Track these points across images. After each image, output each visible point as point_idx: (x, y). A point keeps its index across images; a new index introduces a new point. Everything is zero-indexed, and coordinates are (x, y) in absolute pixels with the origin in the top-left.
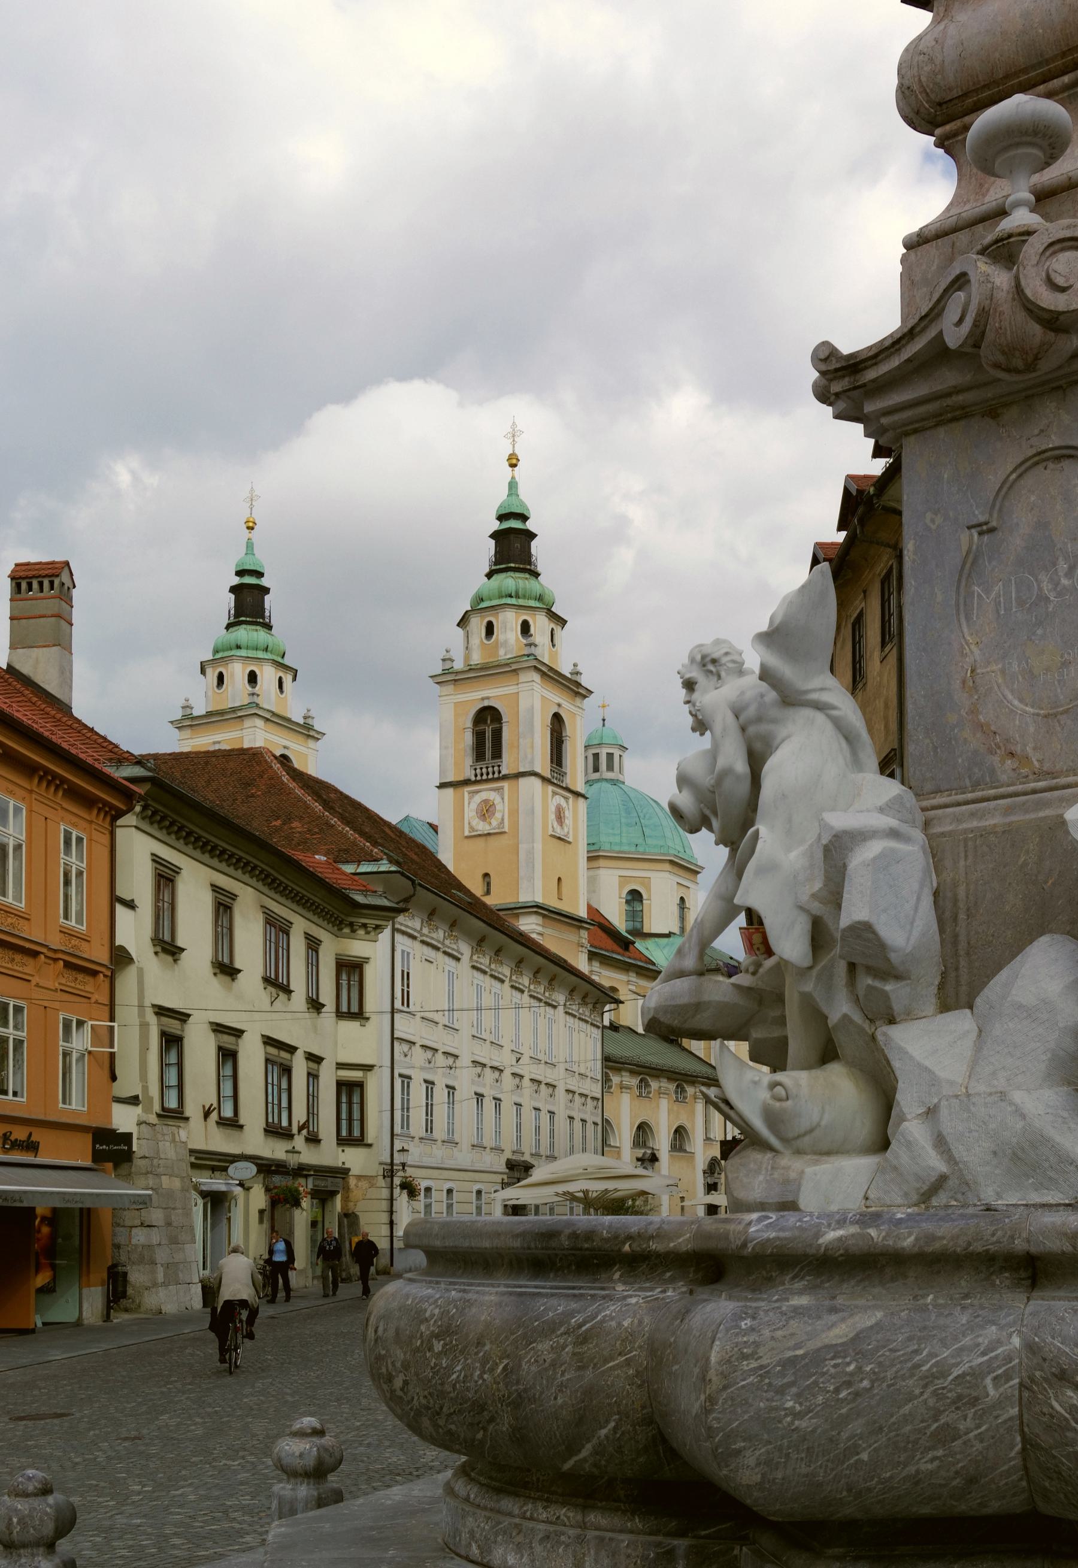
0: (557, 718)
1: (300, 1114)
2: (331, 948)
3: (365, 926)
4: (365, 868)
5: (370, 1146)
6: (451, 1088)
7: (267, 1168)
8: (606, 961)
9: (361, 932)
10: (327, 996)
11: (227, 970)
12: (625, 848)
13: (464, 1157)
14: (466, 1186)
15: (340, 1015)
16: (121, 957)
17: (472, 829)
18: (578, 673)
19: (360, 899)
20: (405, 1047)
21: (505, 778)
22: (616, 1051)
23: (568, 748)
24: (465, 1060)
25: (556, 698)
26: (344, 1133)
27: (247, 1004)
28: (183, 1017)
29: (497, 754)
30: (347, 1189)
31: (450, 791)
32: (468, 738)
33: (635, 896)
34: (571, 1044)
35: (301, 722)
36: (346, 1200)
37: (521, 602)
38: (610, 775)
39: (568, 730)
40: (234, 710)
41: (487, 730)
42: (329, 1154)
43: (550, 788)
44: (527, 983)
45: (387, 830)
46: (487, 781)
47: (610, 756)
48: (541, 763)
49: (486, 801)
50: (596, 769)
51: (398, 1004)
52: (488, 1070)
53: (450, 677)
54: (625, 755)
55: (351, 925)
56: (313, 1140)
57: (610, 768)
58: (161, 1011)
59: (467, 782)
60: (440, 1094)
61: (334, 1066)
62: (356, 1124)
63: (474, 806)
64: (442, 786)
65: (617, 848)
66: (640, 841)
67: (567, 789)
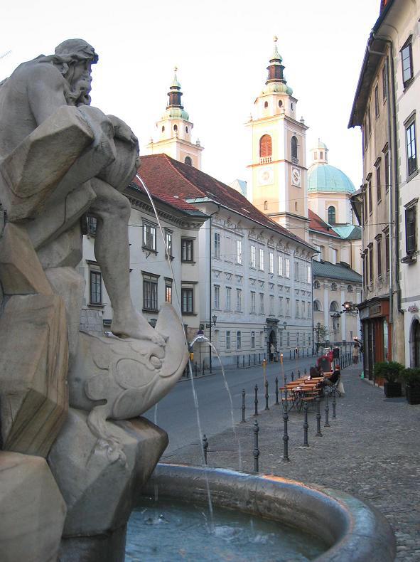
0: (294, 138)
2: (178, 234)
3: (193, 224)
4: (198, 200)
5: (196, 315)
8: (319, 235)
9: (192, 227)
12: (328, 189)
13: (246, 318)
15: (183, 261)
18: (303, 120)
20: (217, 274)
21: (273, 162)
24: (246, 277)
25: (293, 130)
26: (185, 310)
33: (332, 209)
35: (195, 144)
38: (321, 161)
41: (265, 145)
44: (275, 245)
45: (218, 185)
50: (316, 159)
51: (213, 256)
52: (257, 282)
54: (328, 153)
55: (188, 224)
57: (321, 158)
61: (180, 283)
62: (190, 307)
65: (323, 190)
67: (301, 167)
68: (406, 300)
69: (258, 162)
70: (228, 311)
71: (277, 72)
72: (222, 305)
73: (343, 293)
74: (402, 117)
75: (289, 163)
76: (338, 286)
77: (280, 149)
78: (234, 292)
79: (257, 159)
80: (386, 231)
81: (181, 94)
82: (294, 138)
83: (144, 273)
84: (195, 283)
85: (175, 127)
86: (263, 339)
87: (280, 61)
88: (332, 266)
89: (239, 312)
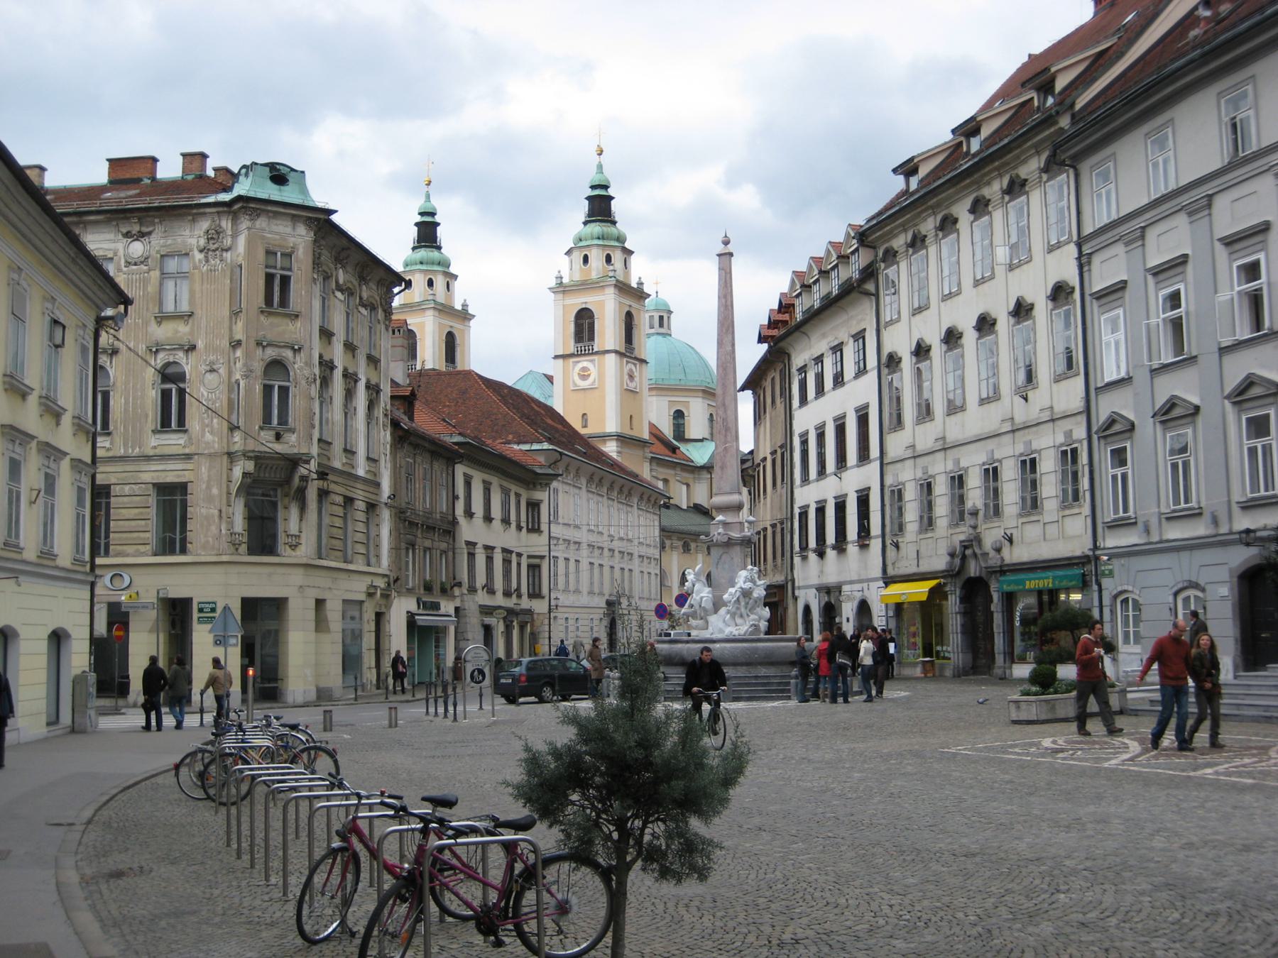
0: (629, 316)
1: (514, 585)
4: (536, 446)
6: (577, 561)
7: (511, 612)
11: (488, 518)
13: (584, 600)
14: (586, 616)
15: (529, 531)
16: (454, 522)
17: (575, 385)
19: (539, 471)
21: (597, 353)
23: (635, 332)
27: (501, 537)
28: (474, 544)
29: (592, 338)
30: (533, 620)
31: (560, 361)
32: (571, 328)
33: (679, 415)
34: (641, 527)
36: (532, 626)
38: (661, 330)
39: (636, 321)
40: (419, 304)
41: (584, 324)
42: (525, 603)
49: (584, 369)
50: (652, 327)
53: (561, 289)
56: (519, 596)
58: (468, 543)
59: (572, 355)
60: (572, 564)
64: (556, 357)
66: (682, 376)
67: (636, 359)
69: (571, 348)
70: (566, 590)
71: (600, 207)
72: (561, 584)
73: (700, 556)
74: (798, 429)
76: (693, 545)
77: (608, 333)
78: (572, 564)
79: (571, 348)
80: (782, 523)
81: (438, 224)
83: (505, 550)
84: (542, 557)
85: (430, 283)
86: (603, 629)
87: (606, 187)
88: (682, 513)
89: (577, 591)
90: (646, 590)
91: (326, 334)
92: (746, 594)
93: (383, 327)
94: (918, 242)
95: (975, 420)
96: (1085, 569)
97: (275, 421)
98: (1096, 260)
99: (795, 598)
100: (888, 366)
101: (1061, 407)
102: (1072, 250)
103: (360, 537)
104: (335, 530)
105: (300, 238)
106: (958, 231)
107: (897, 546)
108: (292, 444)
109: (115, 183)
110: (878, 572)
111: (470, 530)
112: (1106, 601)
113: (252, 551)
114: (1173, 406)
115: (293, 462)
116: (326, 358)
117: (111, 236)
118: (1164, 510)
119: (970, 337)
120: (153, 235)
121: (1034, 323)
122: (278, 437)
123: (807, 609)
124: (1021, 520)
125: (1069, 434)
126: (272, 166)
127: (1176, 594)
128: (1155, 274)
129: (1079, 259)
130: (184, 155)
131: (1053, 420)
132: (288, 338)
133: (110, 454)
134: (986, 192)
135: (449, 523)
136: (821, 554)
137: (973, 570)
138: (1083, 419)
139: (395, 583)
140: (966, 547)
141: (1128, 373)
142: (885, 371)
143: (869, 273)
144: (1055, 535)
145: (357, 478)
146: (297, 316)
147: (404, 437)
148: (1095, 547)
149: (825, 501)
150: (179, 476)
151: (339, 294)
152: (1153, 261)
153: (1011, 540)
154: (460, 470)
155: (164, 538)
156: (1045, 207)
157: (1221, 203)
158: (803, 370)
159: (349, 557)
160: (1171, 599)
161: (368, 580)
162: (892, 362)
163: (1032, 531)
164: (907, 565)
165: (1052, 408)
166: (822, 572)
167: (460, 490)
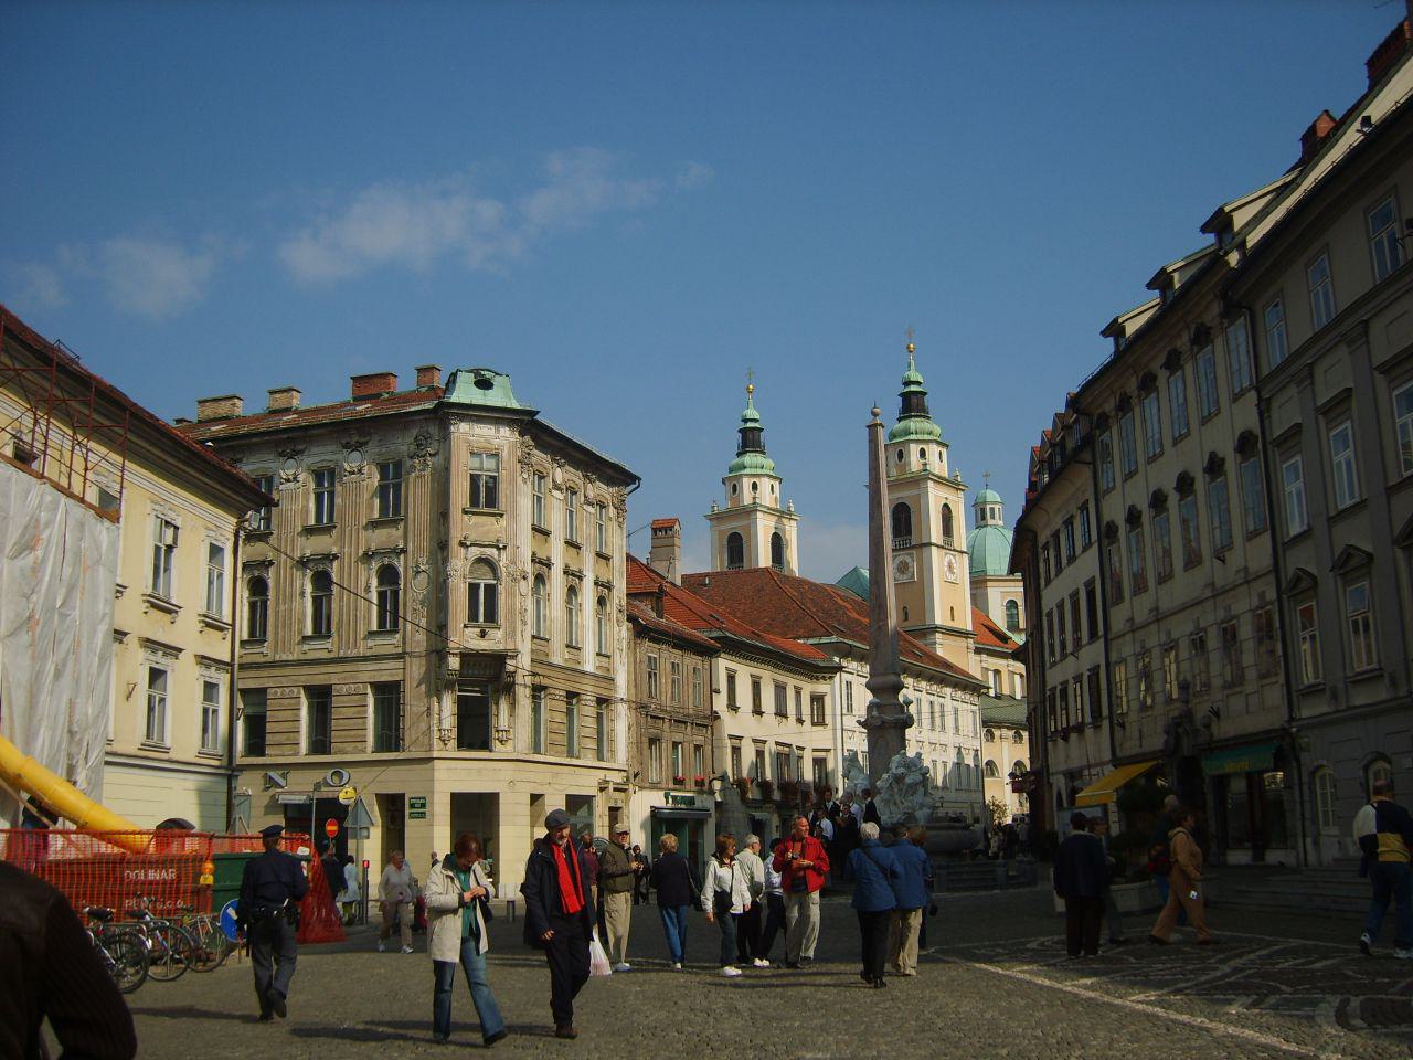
0: (946, 505)
2: (808, 688)
4: (825, 640)
10: (806, 716)
11: (758, 711)
15: (813, 724)
16: (715, 717)
20: (850, 734)
22: (996, 714)
28: (740, 738)
29: (909, 532)
37: (920, 437)
43: (944, 551)
46: (903, 549)
47: (992, 509)
48: (936, 534)
58: (731, 737)
63: (896, 566)
67: (954, 550)
68: (1053, 774)
74: (1045, 612)
75: (938, 546)
82: (946, 505)
84: (828, 750)
90: (964, 781)
91: (541, 532)
92: (899, 779)
93: (616, 525)
94: (1124, 406)
95: (1185, 585)
96: (1282, 746)
97: (481, 619)
98: (1275, 405)
99: (1051, 786)
100: (1107, 537)
101: (1254, 567)
102: (1253, 394)
103: (587, 732)
104: (556, 725)
105: (504, 438)
106: (1157, 389)
107: (1123, 726)
108: (495, 641)
109: (358, 399)
110: (1107, 756)
111: (730, 724)
112: (1305, 779)
113: (461, 745)
114: (1349, 556)
115: (499, 659)
116: (542, 555)
117: (333, 448)
118: (1349, 673)
119: (1173, 499)
120: (370, 444)
121: (1226, 478)
122: (483, 635)
123: (1059, 794)
124: (1226, 692)
125: (1262, 595)
126: (476, 372)
127: (1366, 768)
128: (1325, 413)
129: (1258, 406)
130: (419, 370)
131: (1247, 582)
132: (492, 538)
133: (332, 655)
134: (1178, 344)
135: (705, 717)
136: (1066, 739)
137: (1187, 748)
138: (1272, 577)
139: (636, 778)
140: (1178, 725)
141: (1309, 524)
142: (1105, 542)
143: (1088, 442)
144: (1255, 709)
145: (585, 673)
146: (502, 515)
147: (641, 631)
148: (1292, 719)
149: (1067, 682)
150: (392, 675)
151: (556, 493)
152: (1322, 400)
153: (1217, 714)
154: (723, 664)
155: (382, 735)
156: (1231, 352)
157: (1377, 328)
158: (1046, 547)
159: (576, 751)
160: (1361, 773)
161: (601, 774)
162: (1109, 532)
163: (1236, 703)
164: (1130, 747)
165: (1246, 568)
166: (1068, 756)
167: (723, 685)
